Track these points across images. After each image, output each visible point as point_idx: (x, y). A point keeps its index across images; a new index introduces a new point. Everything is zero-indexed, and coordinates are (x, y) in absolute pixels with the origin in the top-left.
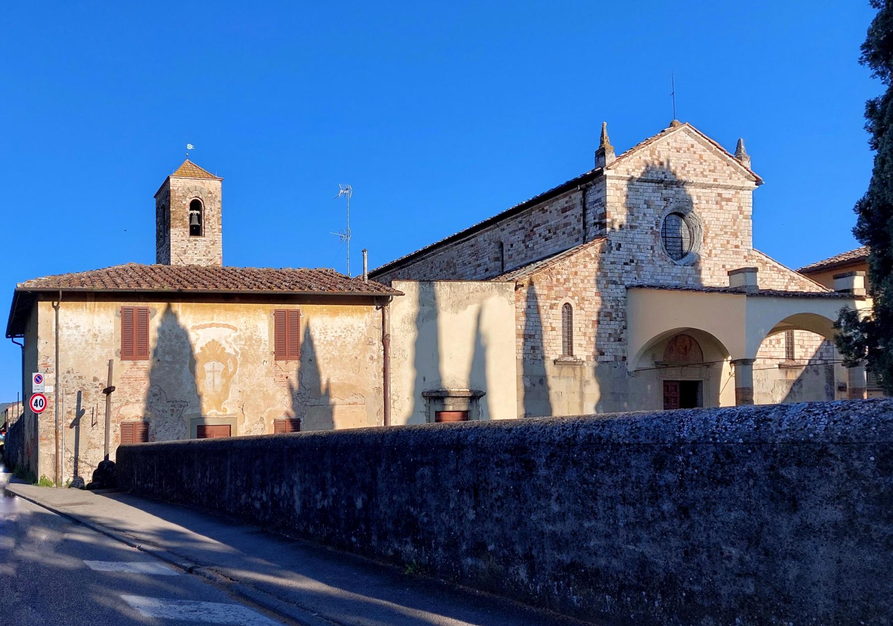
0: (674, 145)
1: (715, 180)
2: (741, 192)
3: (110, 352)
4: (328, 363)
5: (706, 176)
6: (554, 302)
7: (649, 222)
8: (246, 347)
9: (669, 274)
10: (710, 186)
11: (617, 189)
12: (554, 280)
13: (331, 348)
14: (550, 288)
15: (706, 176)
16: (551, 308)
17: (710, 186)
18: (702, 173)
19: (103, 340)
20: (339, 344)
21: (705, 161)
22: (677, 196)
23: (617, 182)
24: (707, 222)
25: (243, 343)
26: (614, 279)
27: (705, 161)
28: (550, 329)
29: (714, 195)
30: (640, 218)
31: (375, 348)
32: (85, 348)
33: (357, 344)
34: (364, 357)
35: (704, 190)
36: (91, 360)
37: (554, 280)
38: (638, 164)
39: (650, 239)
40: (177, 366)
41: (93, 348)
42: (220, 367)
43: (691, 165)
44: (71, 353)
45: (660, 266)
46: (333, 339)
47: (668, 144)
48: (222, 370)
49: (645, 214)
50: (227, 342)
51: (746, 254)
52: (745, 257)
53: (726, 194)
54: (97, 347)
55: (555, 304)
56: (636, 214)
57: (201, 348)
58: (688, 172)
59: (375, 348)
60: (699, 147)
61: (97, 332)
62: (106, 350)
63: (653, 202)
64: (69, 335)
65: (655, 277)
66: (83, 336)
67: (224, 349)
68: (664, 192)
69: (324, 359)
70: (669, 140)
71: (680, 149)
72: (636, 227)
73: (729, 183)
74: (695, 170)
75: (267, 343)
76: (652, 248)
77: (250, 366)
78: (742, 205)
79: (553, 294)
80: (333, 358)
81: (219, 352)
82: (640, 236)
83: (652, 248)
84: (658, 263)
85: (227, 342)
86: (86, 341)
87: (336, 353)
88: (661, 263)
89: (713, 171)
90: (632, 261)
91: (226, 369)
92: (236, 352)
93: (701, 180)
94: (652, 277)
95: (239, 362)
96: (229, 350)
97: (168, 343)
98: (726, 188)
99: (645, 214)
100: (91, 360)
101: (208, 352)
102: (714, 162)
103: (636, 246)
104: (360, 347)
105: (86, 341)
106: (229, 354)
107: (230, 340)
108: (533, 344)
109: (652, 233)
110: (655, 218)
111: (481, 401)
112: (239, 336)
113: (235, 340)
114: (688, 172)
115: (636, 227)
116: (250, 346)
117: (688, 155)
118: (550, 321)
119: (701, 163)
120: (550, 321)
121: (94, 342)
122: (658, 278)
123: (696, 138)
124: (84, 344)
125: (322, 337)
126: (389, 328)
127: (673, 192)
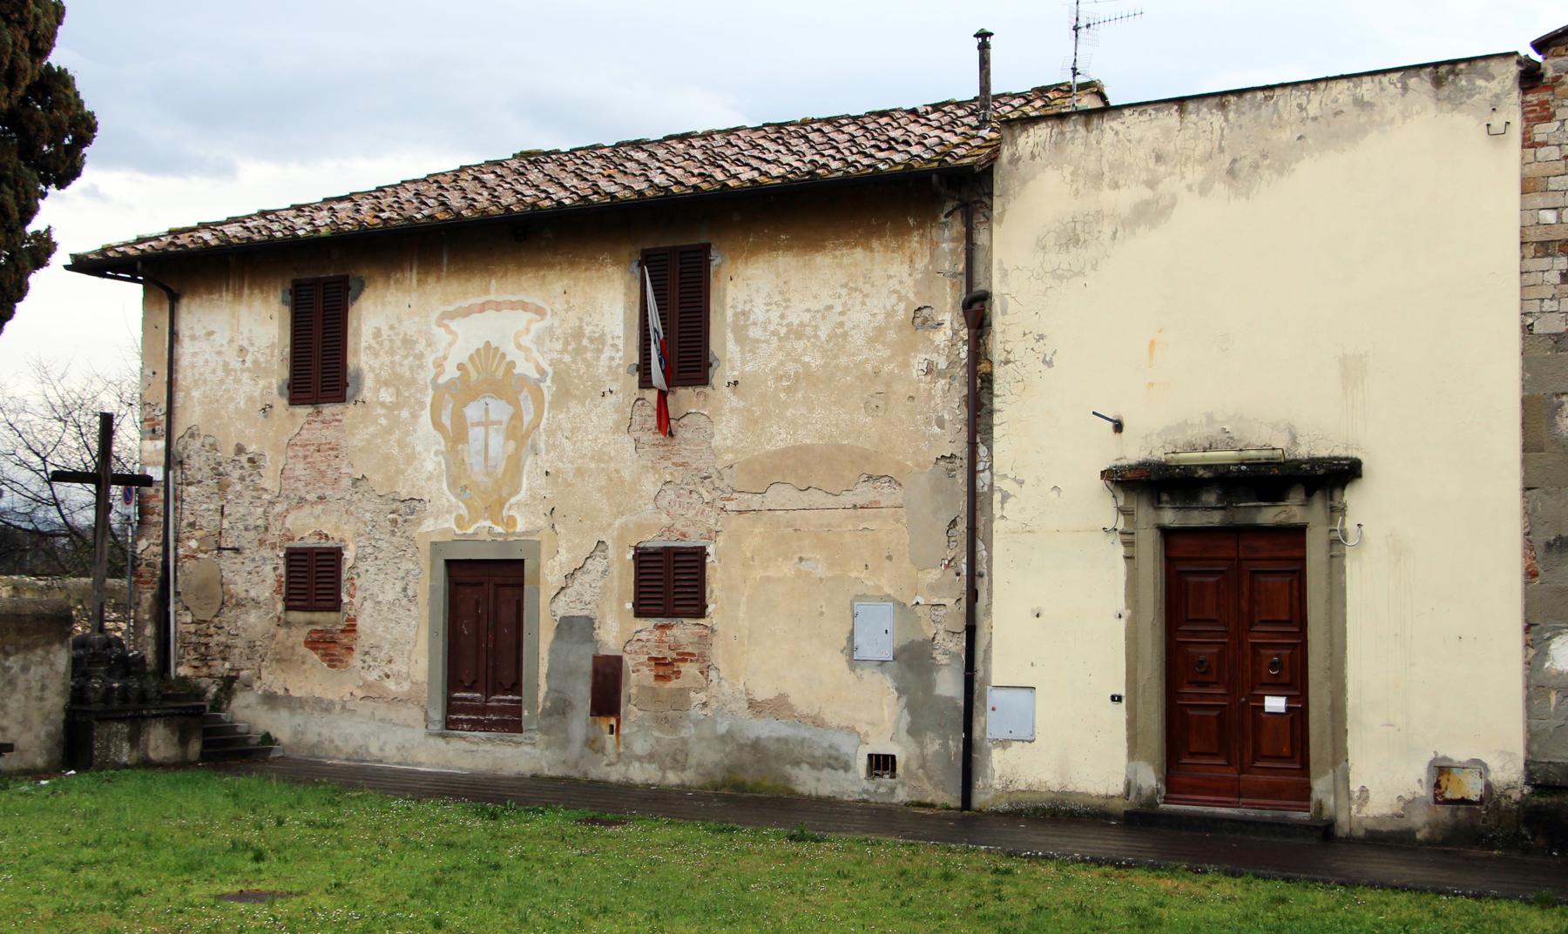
3: (269, 386)
4: (790, 390)
8: (567, 358)
13: (800, 345)
19: (256, 362)
20: (823, 335)
25: (559, 346)
31: (941, 337)
32: (222, 382)
33: (880, 331)
34: (906, 365)
36: (231, 407)
40: (405, 414)
41: (237, 381)
42: (500, 410)
44: (196, 394)
46: (806, 317)
48: (505, 418)
50: (519, 346)
54: (245, 377)
57: (461, 367)
59: (941, 337)
61: (245, 344)
62: (262, 383)
64: (195, 354)
66: (219, 353)
67: (512, 365)
69: (779, 379)
75: (620, 343)
77: (575, 408)
80: (806, 378)
81: (500, 374)
85: (519, 346)
86: (226, 365)
87: (814, 360)
91: (517, 416)
92: (543, 373)
95: (548, 398)
96: (525, 368)
97: (387, 360)
100: (231, 407)
101: (474, 375)
104: (892, 335)
105: (226, 365)
106: (523, 379)
107: (526, 341)
111: (1355, 499)
112: (550, 329)
113: (539, 340)
116: (579, 351)
121: (238, 366)
124: (220, 373)
125: (774, 315)
126: (988, 268)
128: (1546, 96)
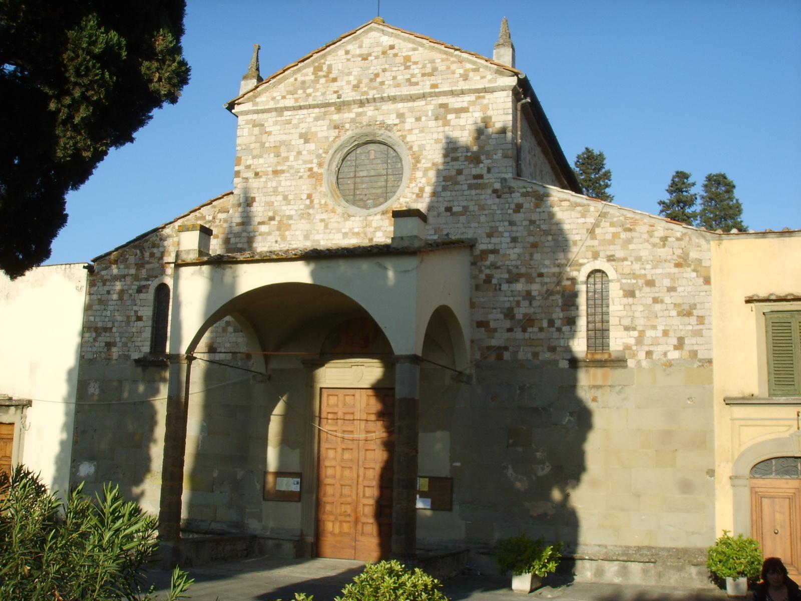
0: (358, 51)
1: (434, 86)
2: (488, 96)
5: (417, 84)
6: (144, 283)
7: (305, 162)
9: (339, 230)
10: (423, 96)
11: (254, 126)
12: (147, 254)
14: (140, 266)
15: (417, 84)
16: (139, 291)
17: (423, 96)
18: (408, 80)
21: (416, 63)
22: (358, 119)
23: (255, 117)
24: (415, 149)
26: (239, 246)
27: (416, 63)
28: (134, 318)
29: (431, 107)
30: (291, 158)
35: (410, 104)
37: (147, 254)
38: (291, 89)
39: (305, 186)
43: (387, 74)
45: (322, 220)
47: (347, 52)
49: (299, 153)
51: (497, 186)
52: (495, 191)
53: (455, 102)
55: (144, 286)
56: (283, 155)
58: (382, 83)
60: (404, 44)
63: (316, 133)
65: (311, 237)
68: (336, 117)
70: (350, 47)
71: (370, 55)
72: (283, 172)
73: (462, 85)
74: (394, 78)
76: (309, 196)
78: (489, 113)
79: (143, 273)
82: (288, 183)
83: (309, 196)
84: (319, 217)
88: (325, 216)
89: (431, 74)
90: (272, 219)
93: (406, 90)
94: (306, 237)
98: (452, 93)
99: (299, 153)
102: (432, 61)
103: (280, 198)
108: (108, 340)
109: (309, 177)
110: (319, 156)
114: (382, 83)
115: (283, 172)
117: (382, 59)
118: (135, 308)
119: (407, 68)
120: (135, 308)
122: (317, 237)
123: (391, 35)
127: (352, 115)
128: (95, 278)
